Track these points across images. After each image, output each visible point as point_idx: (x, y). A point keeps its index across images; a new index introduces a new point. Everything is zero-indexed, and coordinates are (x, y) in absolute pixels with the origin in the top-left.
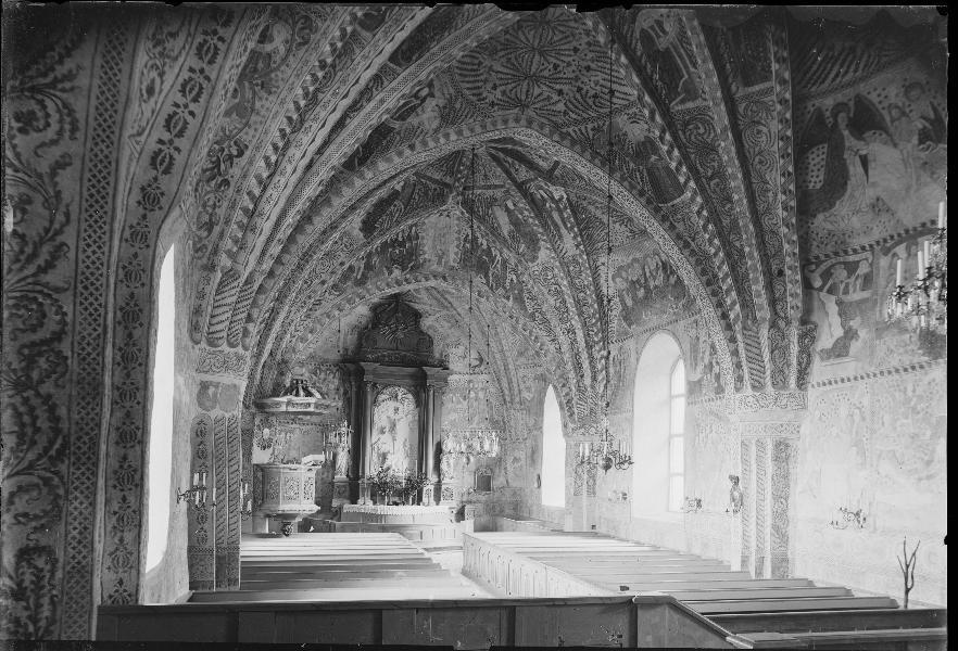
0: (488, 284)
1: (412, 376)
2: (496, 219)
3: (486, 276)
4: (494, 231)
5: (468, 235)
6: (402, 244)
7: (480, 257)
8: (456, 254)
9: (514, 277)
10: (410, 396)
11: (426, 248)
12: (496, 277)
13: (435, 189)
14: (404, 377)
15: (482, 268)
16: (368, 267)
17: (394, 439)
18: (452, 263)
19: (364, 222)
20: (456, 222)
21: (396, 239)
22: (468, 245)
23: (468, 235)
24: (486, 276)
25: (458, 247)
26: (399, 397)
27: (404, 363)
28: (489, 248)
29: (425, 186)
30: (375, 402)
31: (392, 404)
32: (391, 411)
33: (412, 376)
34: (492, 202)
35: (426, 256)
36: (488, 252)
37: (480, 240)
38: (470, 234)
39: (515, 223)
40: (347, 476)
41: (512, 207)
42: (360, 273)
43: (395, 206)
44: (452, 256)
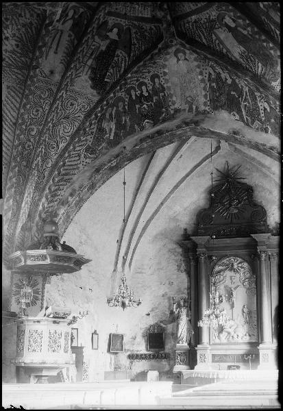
0: (243, 121)
1: (247, 246)
2: (223, 44)
3: (239, 112)
4: (223, 58)
5: (210, 74)
6: (148, 99)
7: (229, 94)
8: (205, 96)
9: (266, 105)
10: (245, 265)
11: (174, 99)
12: (250, 113)
13: (151, 29)
14: (239, 248)
15: (232, 105)
16: (120, 126)
17: (232, 306)
18: (202, 108)
19: (92, 79)
20: (196, 63)
21: (142, 95)
22: (214, 84)
23: (210, 74)
24: (239, 112)
25: (204, 89)
26: (235, 267)
27: (239, 234)
28: (234, 81)
29: (140, 28)
30: (211, 273)
31: (228, 274)
32: (228, 279)
33: (247, 246)
34: (211, 26)
35: (176, 106)
36: (234, 85)
37: (223, 76)
38: (212, 72)
39: (241, 40)
40: (189, 344)
41: (233, 25)
42: (112, 134)
43: (118, 56)
44: (202, 100)
